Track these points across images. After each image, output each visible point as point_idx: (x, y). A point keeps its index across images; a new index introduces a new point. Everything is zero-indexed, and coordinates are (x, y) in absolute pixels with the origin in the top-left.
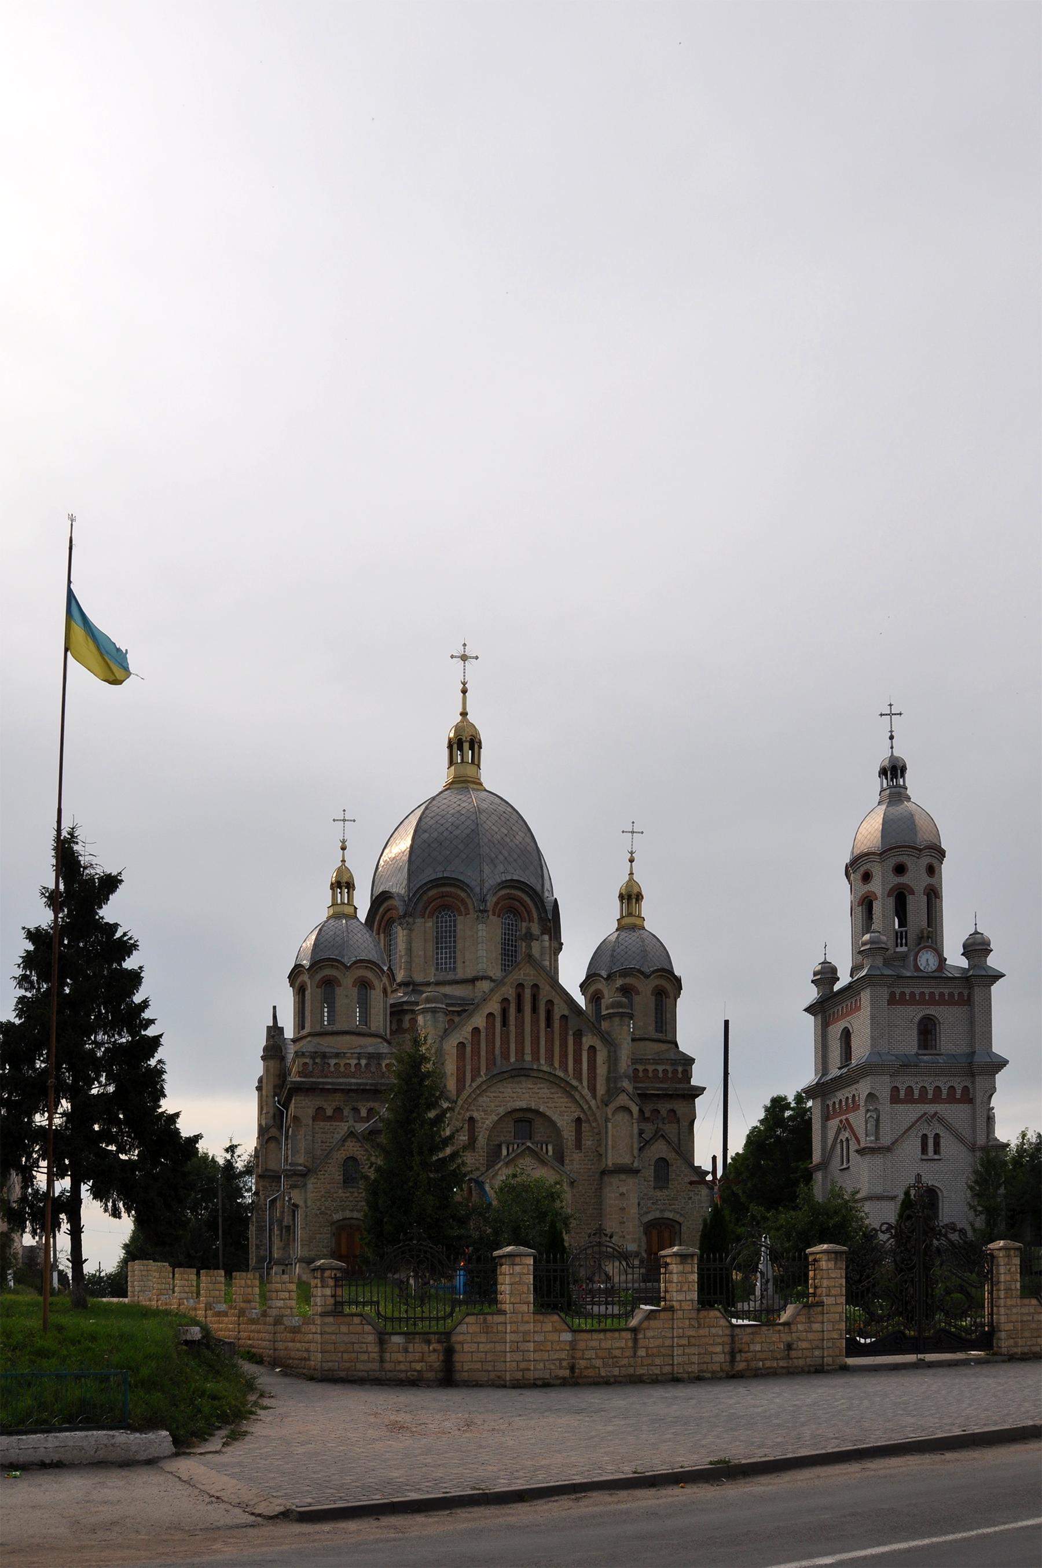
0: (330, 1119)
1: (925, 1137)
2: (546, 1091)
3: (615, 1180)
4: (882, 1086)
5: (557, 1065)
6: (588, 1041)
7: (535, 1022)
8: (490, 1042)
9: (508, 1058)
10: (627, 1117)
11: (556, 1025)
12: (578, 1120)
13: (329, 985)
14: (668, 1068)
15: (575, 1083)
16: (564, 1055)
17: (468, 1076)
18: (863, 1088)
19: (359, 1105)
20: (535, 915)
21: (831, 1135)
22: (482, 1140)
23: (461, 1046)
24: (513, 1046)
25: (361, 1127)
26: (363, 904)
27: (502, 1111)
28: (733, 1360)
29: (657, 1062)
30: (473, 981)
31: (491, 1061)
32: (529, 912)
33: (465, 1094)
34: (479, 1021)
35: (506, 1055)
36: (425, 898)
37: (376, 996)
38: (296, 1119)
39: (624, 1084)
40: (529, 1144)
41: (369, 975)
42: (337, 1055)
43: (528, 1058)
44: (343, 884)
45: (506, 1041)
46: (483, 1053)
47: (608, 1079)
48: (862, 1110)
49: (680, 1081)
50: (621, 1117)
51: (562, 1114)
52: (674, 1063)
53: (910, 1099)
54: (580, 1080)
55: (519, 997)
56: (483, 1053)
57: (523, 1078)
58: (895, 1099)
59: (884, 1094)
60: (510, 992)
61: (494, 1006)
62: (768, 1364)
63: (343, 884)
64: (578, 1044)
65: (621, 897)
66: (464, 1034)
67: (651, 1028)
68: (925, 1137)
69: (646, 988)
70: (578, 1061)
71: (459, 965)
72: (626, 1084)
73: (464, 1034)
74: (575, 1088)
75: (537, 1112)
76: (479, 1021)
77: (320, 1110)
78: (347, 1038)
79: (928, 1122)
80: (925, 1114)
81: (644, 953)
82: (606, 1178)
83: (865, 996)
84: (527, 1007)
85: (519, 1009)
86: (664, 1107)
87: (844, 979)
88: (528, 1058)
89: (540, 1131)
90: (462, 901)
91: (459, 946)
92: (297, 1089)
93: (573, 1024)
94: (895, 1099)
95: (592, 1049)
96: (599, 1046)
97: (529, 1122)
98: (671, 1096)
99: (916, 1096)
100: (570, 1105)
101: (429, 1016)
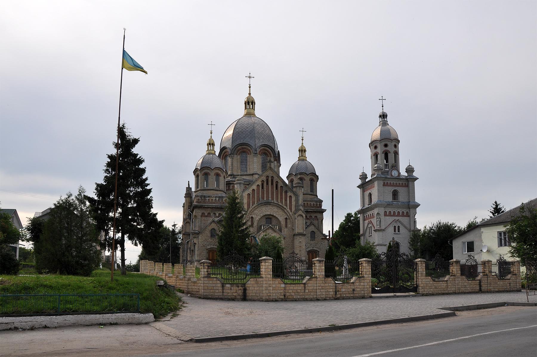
0: (206, 216)
1: (395, 227)
3: (298, 237)
4: (382, 211)
6: (289, 194)
7: (272, 188)
8: (258, 194)
10: (302, 218)
11: (279, 189)
13: (206, 175)
15: (285, 207)
16: (282, 198)
17: (251, 204)
18: (375, 211)
19: (216, 212)
21: (366, 225)
22: (255, 224)
23: (249, 194)
24: (265, 195)
25: (216, 219)
26: (217, 150)
27: (262, 215)
28: (336, 294)
29: (311, 201)
30: (253, 175)
31: (258, 200)
32: (270, 154)
34: (254, 187)
35: (263, 198)
37: (221, 178)
38: (195, 216)
41: (219, 172)
42: (209, 197)
43: (270, 199)
44: (211, 144)
45: (263, 193)
46: (256, 197)
47: (295, 206)
48: (375, 218)
49: (318, 207)
50: (300, 218)
51: (281, 216)
52: (316, 202)
53: (390, 215)
55: (267, 180)
56: (256, 197)
58: (385, 215)
59: (382, 213)
60: (264, 178)
61: (259, 183)
62: (347, 295)
63: (211, 144)
64: (286, 195)
65: (299, 151)
66: (250, 191)
67: (309, 191)
68: (395, 227)
69: (307, 178)
70: (286, 200)
71: (248, 170)
72: (301, 208)
73: (250, 191)
75: (273, 216)
76: (254, 187)
77: (203, 214)
78: (212, 191)
79: (396, 222)
81: (307, 167)
82: (295, 237)
83: (376, 183)
84: (270, 183)
85: (267, 184)
86: (313, 215)
87: (369, 178)
88: (270, 199)
89: (274, 222)
90: (249, 150)
91: (248, 164)
92: (196, 207)
94: (385, 215)
95: (290, 196)
96: (292, 195)
97: (271, 219)
101: (238, 185)
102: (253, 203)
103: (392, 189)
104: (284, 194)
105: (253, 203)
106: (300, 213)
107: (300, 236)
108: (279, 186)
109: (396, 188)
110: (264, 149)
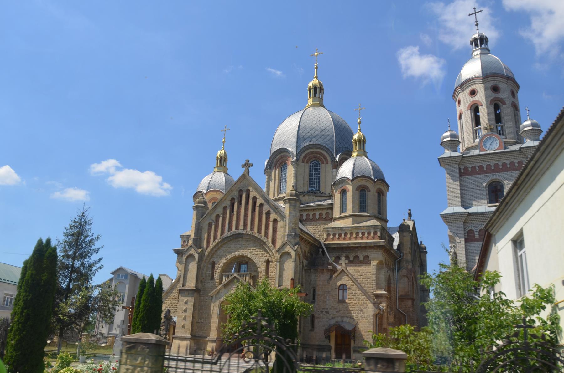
6: (273, 216)
11: (257, 209)
32: (326, 159)
33: (209, 249)
40: (236, 275)
43: (241, 227)
57: (240, 239)
74: (265, 243)
85: (240, 203)
88: (241, 227)
93: (266, 208)
95: (275, 221)
98: (365, 247)
100: (264, 252)
102: (215, 238)
103: (484, 181)
104: (264, 216)
105: (215, 238)
108: (258, 204)
109: (496, 176)
110: (312, 153)
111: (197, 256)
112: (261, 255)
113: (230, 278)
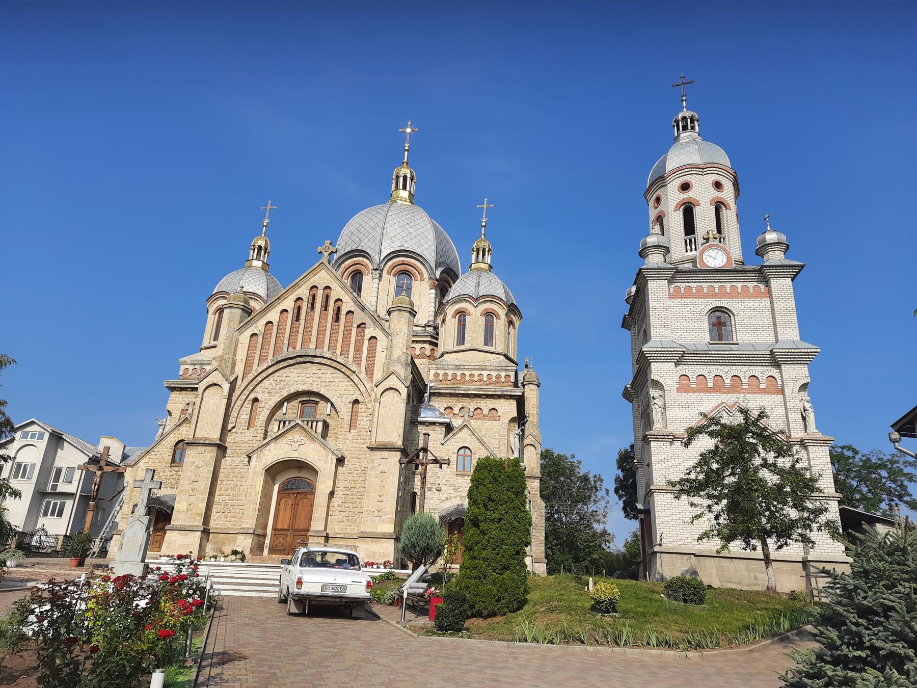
2: (329, 375)
5: (338, 352)
6: (369, 332)
9: (294, 348)
11: (343, 317)
12: (356, 402)
14: (491, 373)
20: (426, 276)
34: (273, 315)
36: (343, 266)
39: (396, 369)
40: (299, 421)
43: (313, 346)
53: (702, 386)
54: (359, 365)
58: (684, 385)
61: (288, 304)
66: (259, 326)
70: (358, 349)
80: (722, 403)
93: (359, 317)
99: (710, 385)
100: (350, 388)
106: (393, 381)
107: (385, 454)
108: (344, 311)
111: (226, 386)
112: (343, 392)
113: (288, 426)
